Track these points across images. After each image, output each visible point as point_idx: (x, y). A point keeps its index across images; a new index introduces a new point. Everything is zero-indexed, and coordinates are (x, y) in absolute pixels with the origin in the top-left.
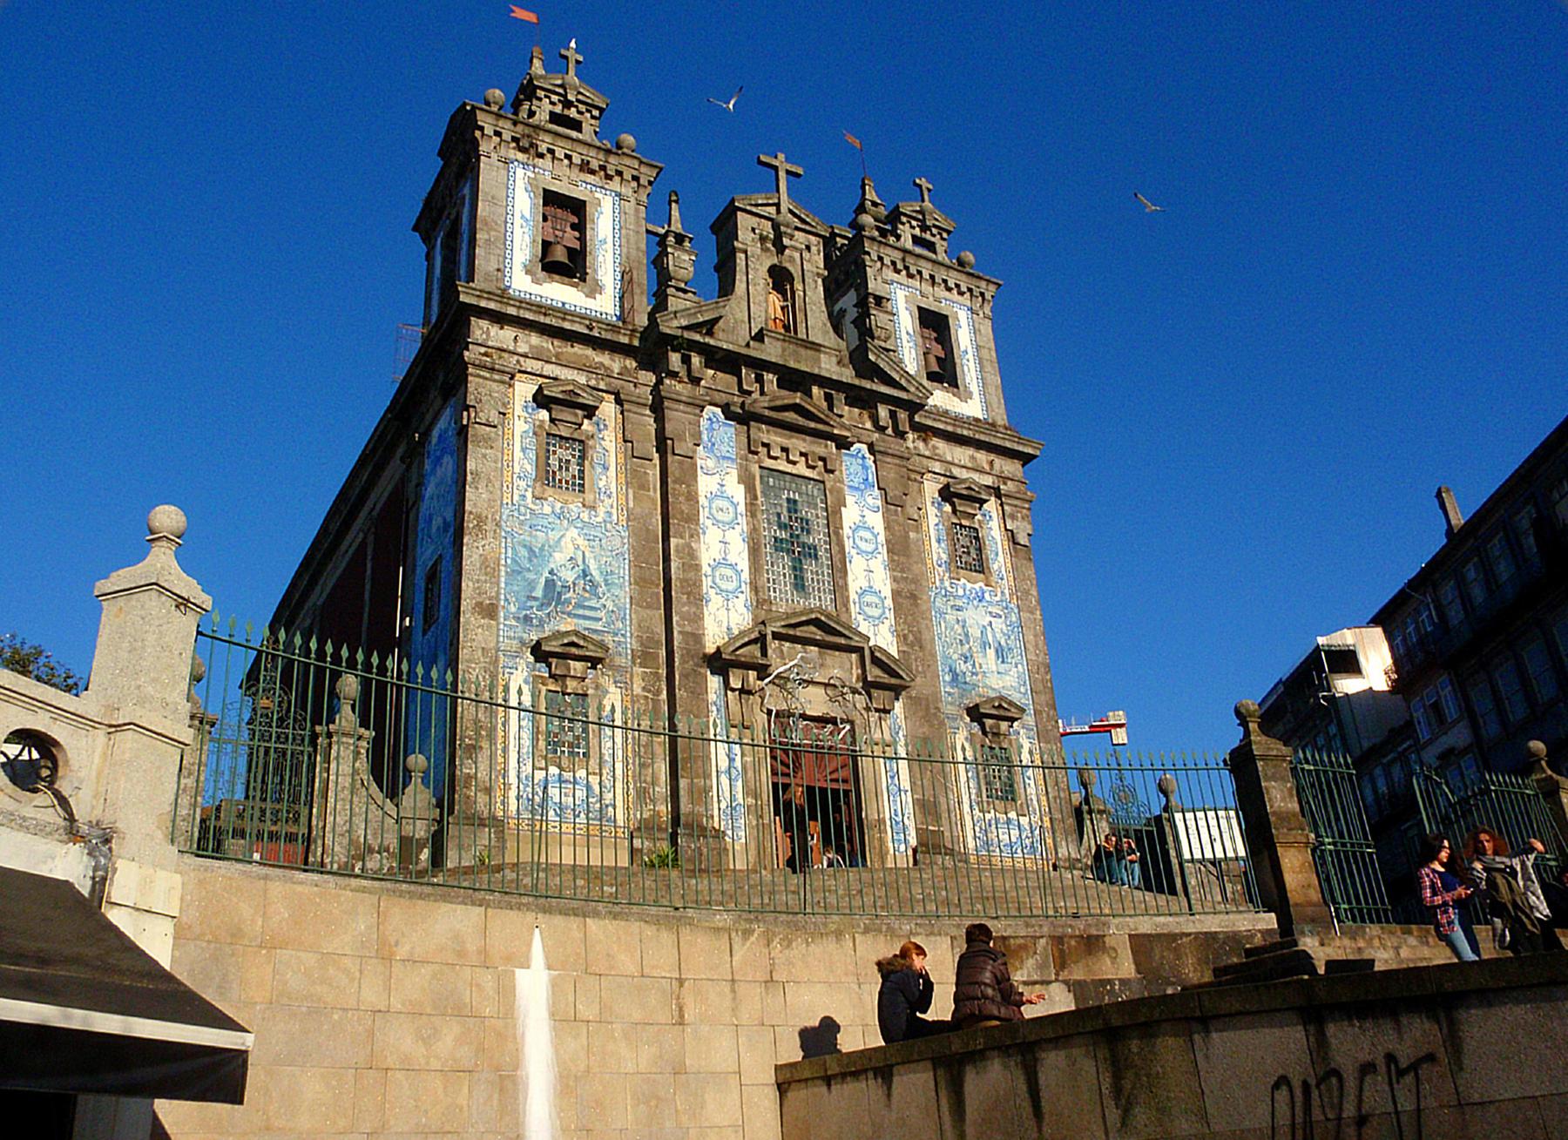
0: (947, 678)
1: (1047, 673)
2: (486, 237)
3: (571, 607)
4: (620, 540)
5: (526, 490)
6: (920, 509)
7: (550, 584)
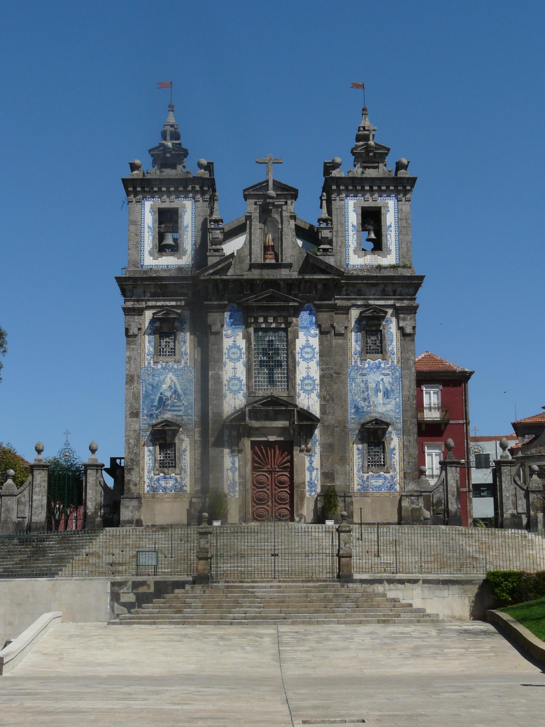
0: (353, 411)
1: (413, 400)
2: (132, 243)
3: (169, 407)
4: (192, 375)
5: (151, 360)
6: (347, 327)
7: (161, 399)
